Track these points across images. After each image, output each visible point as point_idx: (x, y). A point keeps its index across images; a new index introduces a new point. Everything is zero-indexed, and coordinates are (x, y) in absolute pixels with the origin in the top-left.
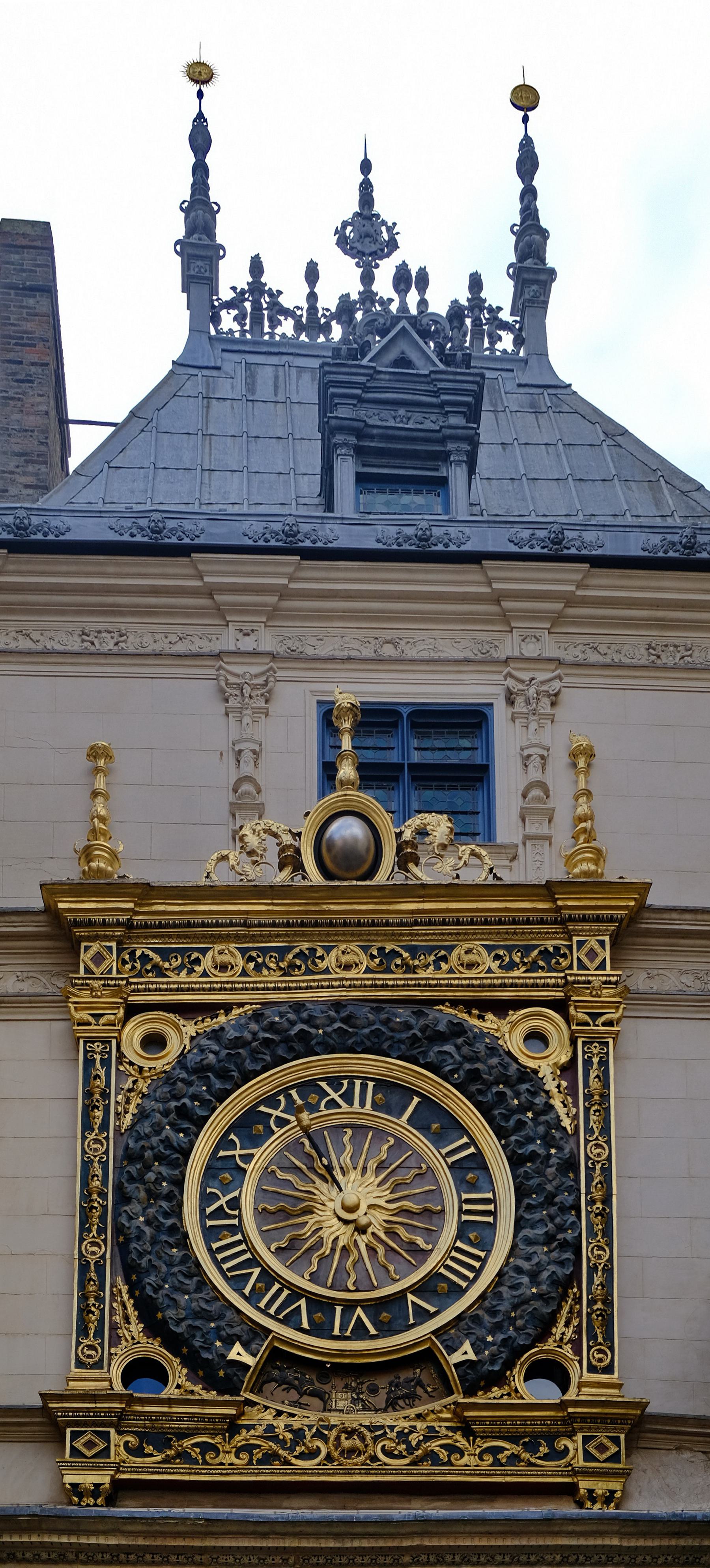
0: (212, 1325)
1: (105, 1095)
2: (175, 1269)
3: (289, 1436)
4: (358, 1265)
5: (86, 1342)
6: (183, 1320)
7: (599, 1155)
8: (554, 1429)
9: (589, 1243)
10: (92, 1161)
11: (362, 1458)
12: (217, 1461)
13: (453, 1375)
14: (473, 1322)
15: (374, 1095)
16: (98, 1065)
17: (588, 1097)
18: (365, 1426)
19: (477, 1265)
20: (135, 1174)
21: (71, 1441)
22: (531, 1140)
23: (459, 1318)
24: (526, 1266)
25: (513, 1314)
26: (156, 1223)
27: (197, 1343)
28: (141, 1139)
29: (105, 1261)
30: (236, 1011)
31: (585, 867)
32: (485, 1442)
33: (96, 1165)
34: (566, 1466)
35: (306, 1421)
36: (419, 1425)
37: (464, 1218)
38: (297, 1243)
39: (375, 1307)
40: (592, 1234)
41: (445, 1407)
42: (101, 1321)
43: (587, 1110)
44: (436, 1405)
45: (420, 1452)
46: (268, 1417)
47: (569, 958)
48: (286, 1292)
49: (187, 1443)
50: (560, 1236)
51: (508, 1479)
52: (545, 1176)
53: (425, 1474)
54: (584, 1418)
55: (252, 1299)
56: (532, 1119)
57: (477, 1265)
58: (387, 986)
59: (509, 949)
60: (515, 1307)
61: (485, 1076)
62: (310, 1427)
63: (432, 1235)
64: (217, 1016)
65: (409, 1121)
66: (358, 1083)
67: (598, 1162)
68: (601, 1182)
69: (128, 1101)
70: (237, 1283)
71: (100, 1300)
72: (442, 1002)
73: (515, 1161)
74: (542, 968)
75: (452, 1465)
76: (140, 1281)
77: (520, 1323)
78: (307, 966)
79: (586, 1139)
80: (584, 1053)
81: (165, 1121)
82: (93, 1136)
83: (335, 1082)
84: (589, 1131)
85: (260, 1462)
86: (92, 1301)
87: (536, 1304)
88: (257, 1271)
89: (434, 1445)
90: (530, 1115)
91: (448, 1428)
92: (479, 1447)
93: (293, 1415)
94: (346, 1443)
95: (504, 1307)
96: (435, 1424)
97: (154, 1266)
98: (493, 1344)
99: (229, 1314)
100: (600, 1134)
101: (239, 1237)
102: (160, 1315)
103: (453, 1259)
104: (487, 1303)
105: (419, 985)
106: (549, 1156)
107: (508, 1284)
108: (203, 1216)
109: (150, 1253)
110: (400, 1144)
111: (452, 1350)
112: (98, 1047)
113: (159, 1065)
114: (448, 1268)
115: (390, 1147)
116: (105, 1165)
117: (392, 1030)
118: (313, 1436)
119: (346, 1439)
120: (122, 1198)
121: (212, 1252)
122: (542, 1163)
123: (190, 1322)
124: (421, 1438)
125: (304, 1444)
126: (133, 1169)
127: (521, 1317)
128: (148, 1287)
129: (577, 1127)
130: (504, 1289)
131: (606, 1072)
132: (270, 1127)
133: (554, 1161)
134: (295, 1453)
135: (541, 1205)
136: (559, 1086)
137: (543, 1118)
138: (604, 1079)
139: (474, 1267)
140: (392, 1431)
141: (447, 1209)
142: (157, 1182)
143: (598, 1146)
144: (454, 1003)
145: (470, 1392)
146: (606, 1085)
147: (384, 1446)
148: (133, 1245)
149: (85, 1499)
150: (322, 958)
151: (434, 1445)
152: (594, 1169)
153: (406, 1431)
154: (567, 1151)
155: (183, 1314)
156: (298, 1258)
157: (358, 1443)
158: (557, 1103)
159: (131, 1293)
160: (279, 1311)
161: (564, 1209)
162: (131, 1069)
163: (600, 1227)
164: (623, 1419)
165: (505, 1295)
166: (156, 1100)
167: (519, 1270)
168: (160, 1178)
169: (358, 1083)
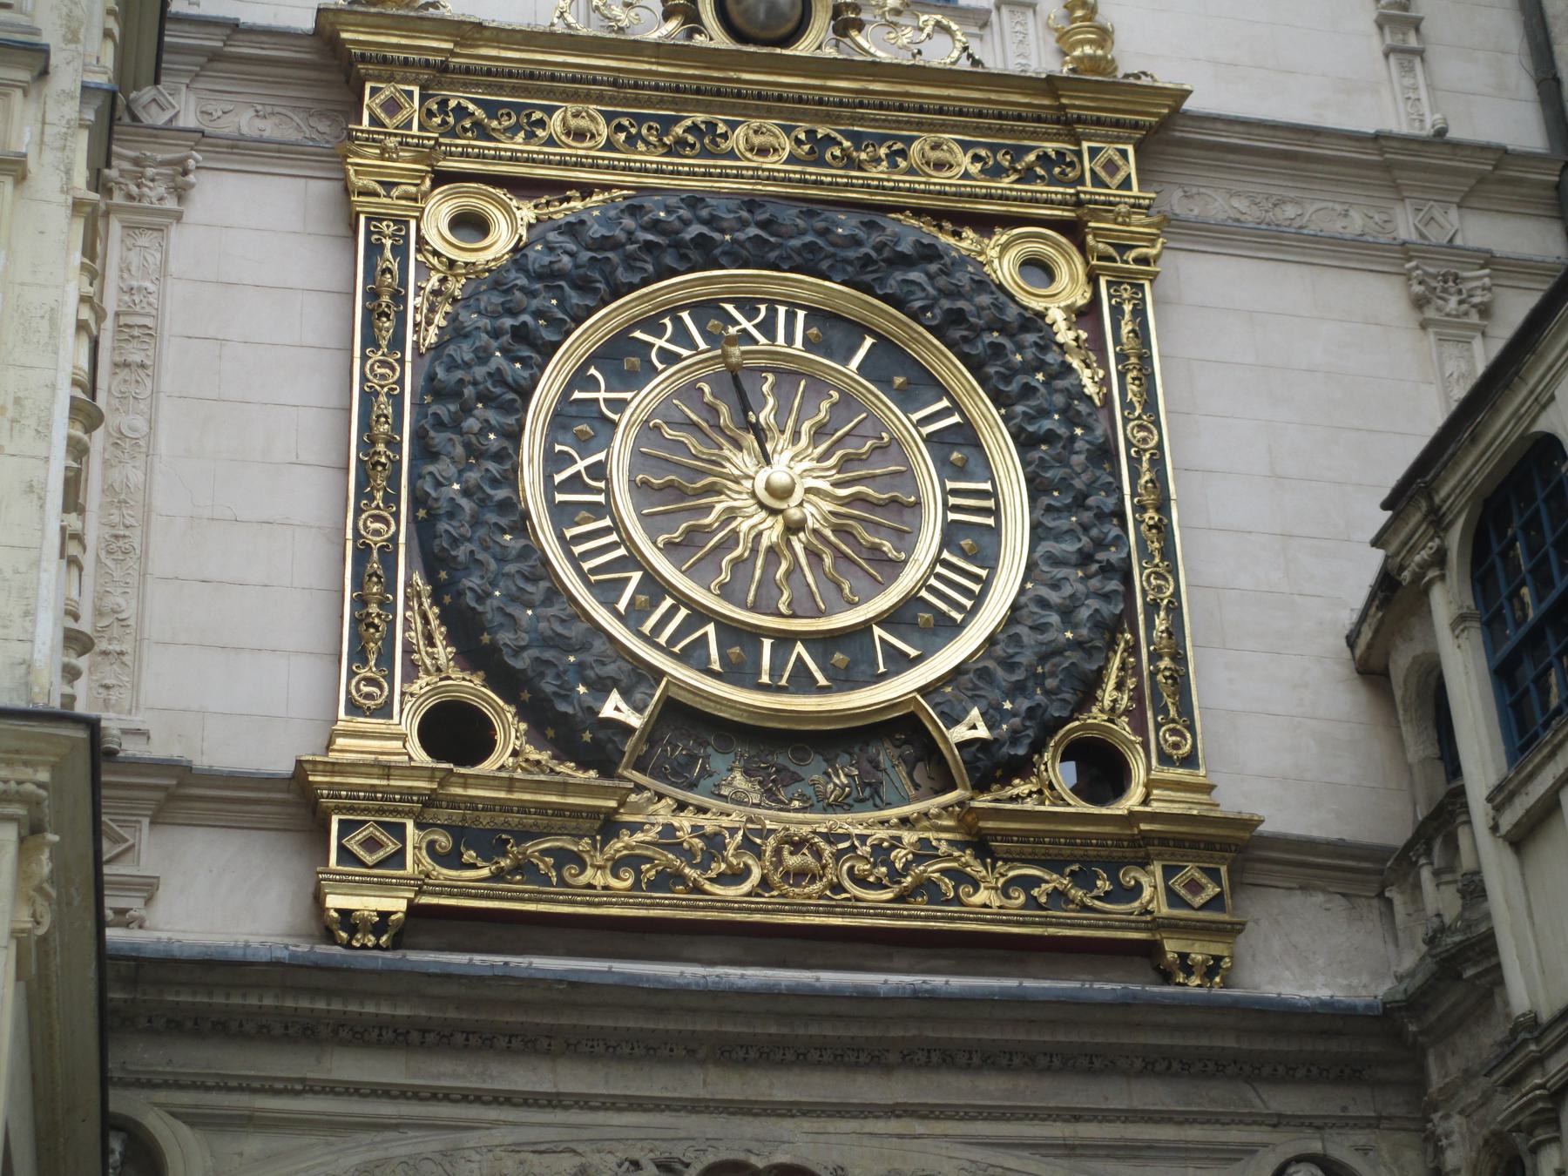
0: (572, 659)
1: (399, 298)
2: (511, 568)
3: (699, 844)
4: (794, 576)
5: (364, 672)
6: (523, 648)
7: (1144, 440)
8: (1117, 853)
9: (1142, 569)
10: (377, 394)
11: (818, 886)
12: (583, 880)
13: (954, 758)
14: (980, 677)
15: (805, 329)
16: (388, 254)
17: (1122, 357)
18: (820, 834)
19: (976, 588)
20: (446, 418)
21: (340, 838)
22: (1044, 413)
23: (958, 670)
24: (1054, 597)
25: (1040, 670)
26: (480, 495)
27: (549, 685)
28: (457, 367)
29: (396, 546)
30: (597, 198)
31: (1088, 50)
32: (1011, 869)
33: (383, 399)
34: (1141, 914)
35: (725, 822)
36: (909, 837)
37: (952, 516)
38: (698, 537)
39: (822, 643)
40: (1145, 554)
41: (945, 808)
42: (390, 639)
43: (1122, 376)
44: (933, 804)
45: (909, 879)
46: (662, 813)
47: (1078, 166)
48: (683, 612)
49: (532, 848)
50: (1101, 556)
51: (1051, 931)
52: (1070, 467)
53: (920, 917)
54: (1163, 840)
56: (1044, 383)
57: (976, 588)
58: (822, 183)
59: (994, 148)
60: (1043, 659)
61: (972, 320)
62: (733, 831)
63: (906, 538)
64: (568, 199)
65: (861, 369)
66: (782, 310)
67: (1145, 450)
68: (1151, 481)
69: (432, 309)
70: (607, 592)
71: (388, 606)
72: (900, 209)
73: (1025, 442)
74: (1042, 178)
75: (963, 905)
76: (452, 582)
77: (1051, 683)
78: (703, 145)
79: (1124, 418)
80: (1110, 297)
81: (495, 344)
82: (378, 356)
84: (1127, 406)
85: (652, 886)
86: (374, 609)
87: (1073, 656)
88: (636, 576)
89: (932, 870)
90: (1040, 376)
91: (950, 842)
92: (1002, 875)
93: (702, 810)
94: (792, 861)
95: (1026, 658)
96: (930, 835)
97: (477, 561)
98: (1013, 713)
99: (599, 645)
100: (1144, 411)
101: (607, 522)
102: (486, 638)
103: (939, 577)
104: (999, 650)
105: (869, 186)
106: (1073, 438)
107: (1029, 623)
108: (550, 488)
109: (469, 540)
110: (848, 403)
111: (953, 721)
112: (387, 227)
113: (480, 258)
114: (932, 590)
115: (833, 405)
116: (397, 401)
117: (833, 245)
118: (738, 848)
119: (792, 853)
120: (425, 451)
122: (1064, 447)
123: (534, 652)
124: (910, 857)
125: (725, 860)
126: (445, 410)
127: (1053, 674)
128: (469, 594)
129: (1108, 399)
130: (1022, 630)
131: (1144, 324)
132: (650, 362)
133: (1078, 445)
134: (713, 874)
135: (1068, 509)
136: (1077, 339)
137: (1059, 384)
138: (1141, 333)
139: (972, 592)
140: (863, 843)
141: (924, 500)
142: (483, 432)
143: (1141, 427)
144: (918, 212)
145: (981, 786)
146: (1146, 343)
147: (851, 868)
148: (443, 526)
149: (359, 936)
150: (725, 136)
151: (932, 870)
152: (1139, 460)
153: (885, 844)
154: (1099, 432)
155: (525, 639)
156: (699, 560)
157: (810, 859)
158: (1076, 364)
159: (436, 599)
160: (673, 640)
161: (1101, 516)
162: (435, 261)
163: (1156, 545)
165: (1025, 639)
166: (480, 313)
167: (1043, 603)
168: (487, 427)
169: (782, 310)
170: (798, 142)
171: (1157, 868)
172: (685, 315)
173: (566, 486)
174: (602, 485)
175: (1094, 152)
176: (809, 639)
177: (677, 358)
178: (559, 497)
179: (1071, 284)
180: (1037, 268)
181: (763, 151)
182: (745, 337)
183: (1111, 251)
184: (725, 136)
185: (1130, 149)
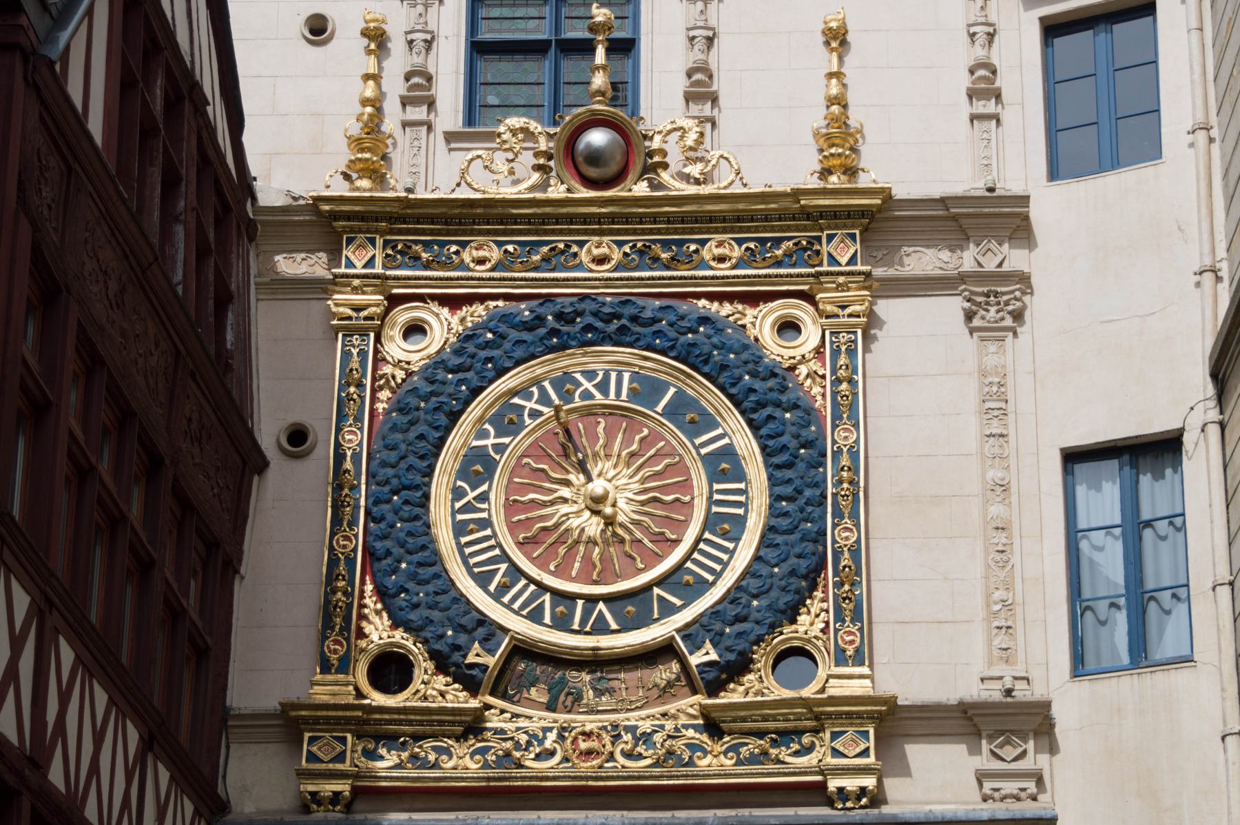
37: (715, 509)
55: (497, 597)
70: (482, 580)
83: (590, 375)
88: (504, 567)
94: (583, 746)
101: (488, 532)
111: (696, 647)
121: (461, 548)
145: (714, 689)
160: (523, 607)
164: (871, 717)
169: (613, 375)
170: (626, 254)
171: (827, 736)
172: (546, 384)
173: (463, 510)
174: (485, 506)
175: (830, 238)
176: (609, 599)
177: (541, 414)
178: (460, 517)
179: (811, 336)
180: (788, 327)
181: (601, 260)
182: (587, 395)
183: (836, 310)
184: (575, 255)
185: (857, 232)
